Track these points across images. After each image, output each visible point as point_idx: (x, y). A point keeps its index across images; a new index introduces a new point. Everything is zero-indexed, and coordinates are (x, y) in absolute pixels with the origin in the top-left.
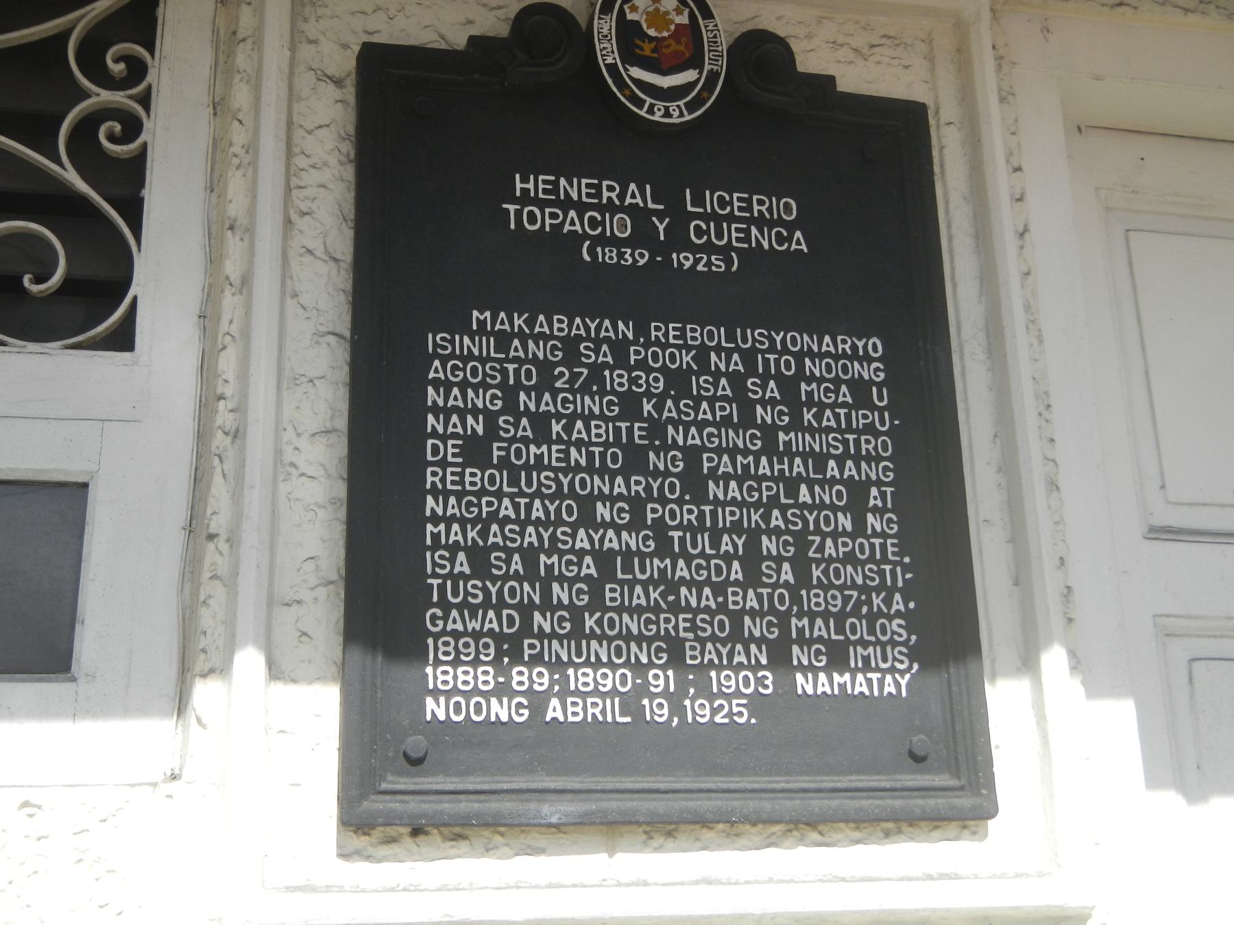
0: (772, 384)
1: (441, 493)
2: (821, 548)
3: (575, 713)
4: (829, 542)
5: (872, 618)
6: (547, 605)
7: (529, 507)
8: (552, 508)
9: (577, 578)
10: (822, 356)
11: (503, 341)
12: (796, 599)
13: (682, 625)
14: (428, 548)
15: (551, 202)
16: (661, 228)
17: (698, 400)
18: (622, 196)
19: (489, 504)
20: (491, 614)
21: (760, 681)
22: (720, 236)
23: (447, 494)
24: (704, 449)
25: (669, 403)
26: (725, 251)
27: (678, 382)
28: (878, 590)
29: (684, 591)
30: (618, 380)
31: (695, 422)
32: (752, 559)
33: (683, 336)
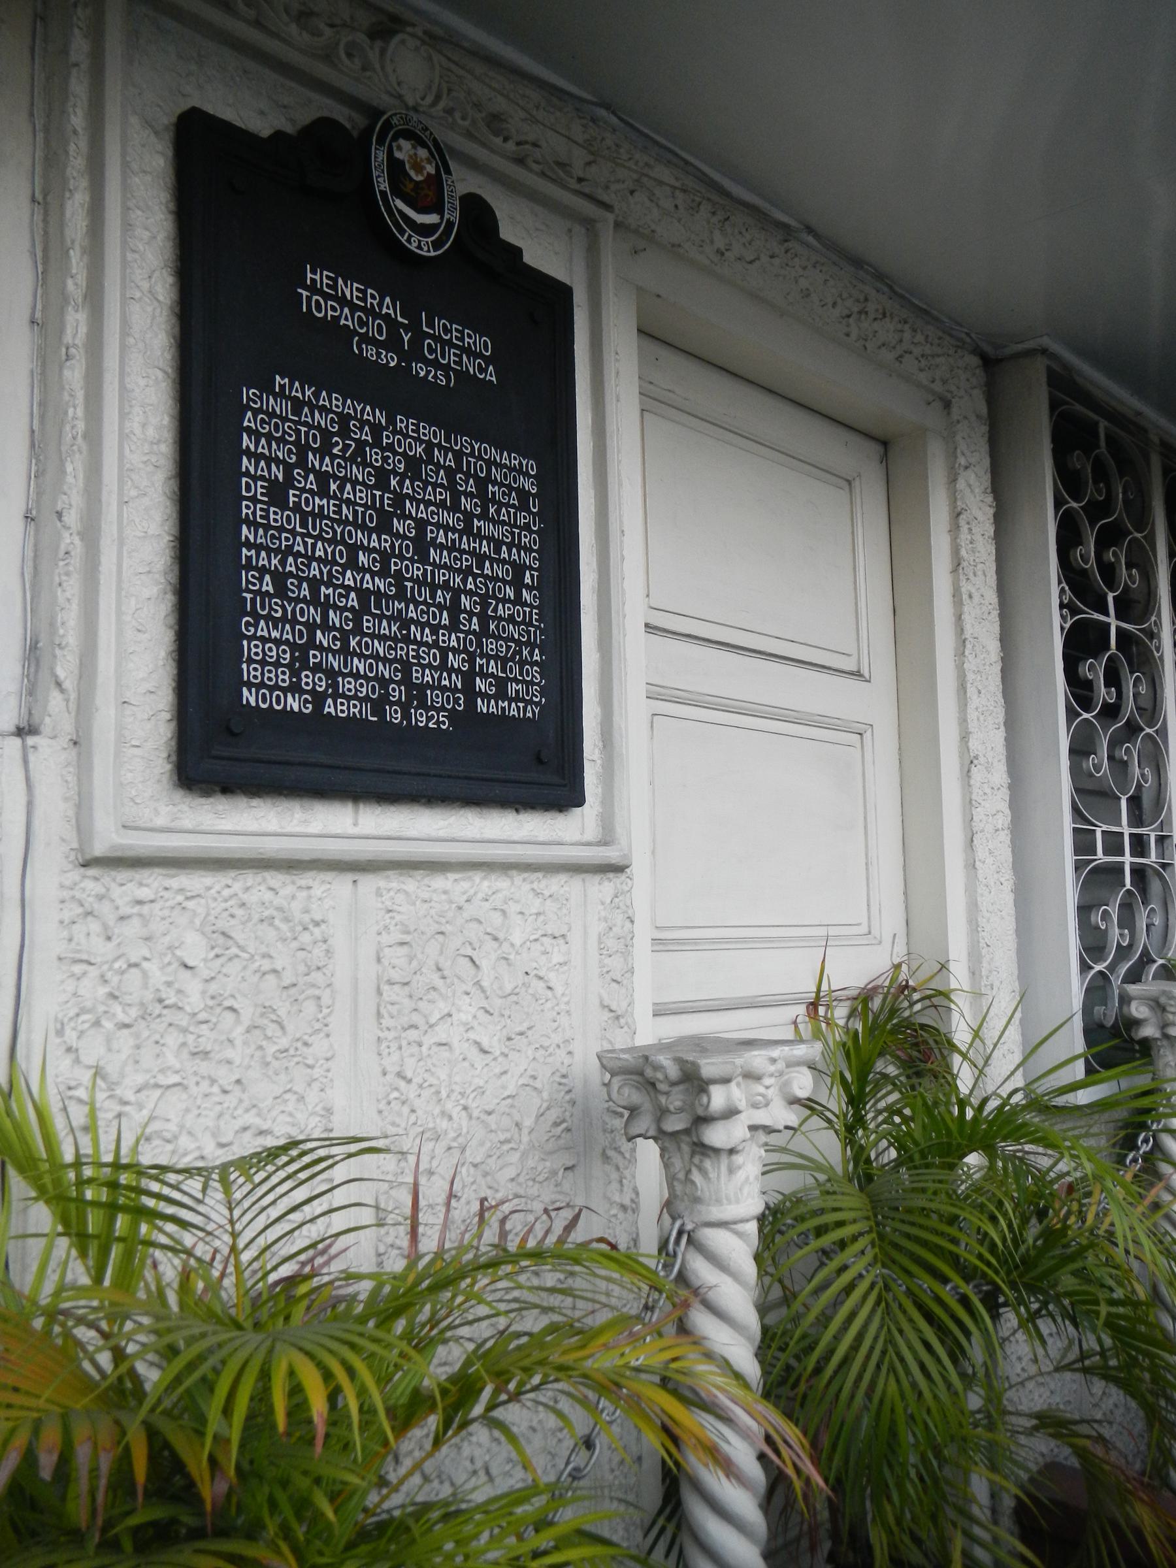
1: (252, 524)
2: (495, 610)
5: (522, 663)
6: (326, 627)
11: (297, 406)
12: (480, 645)
14: (243, 567)
17: (426, 483)
19: (287, 539)
20: (288, 627)
21: (456, 700)
26: (446, 368)
27: (414, 465)
30: (374, 456)
31: (423, 500)
32: (455, 609)
33: (417, 431)
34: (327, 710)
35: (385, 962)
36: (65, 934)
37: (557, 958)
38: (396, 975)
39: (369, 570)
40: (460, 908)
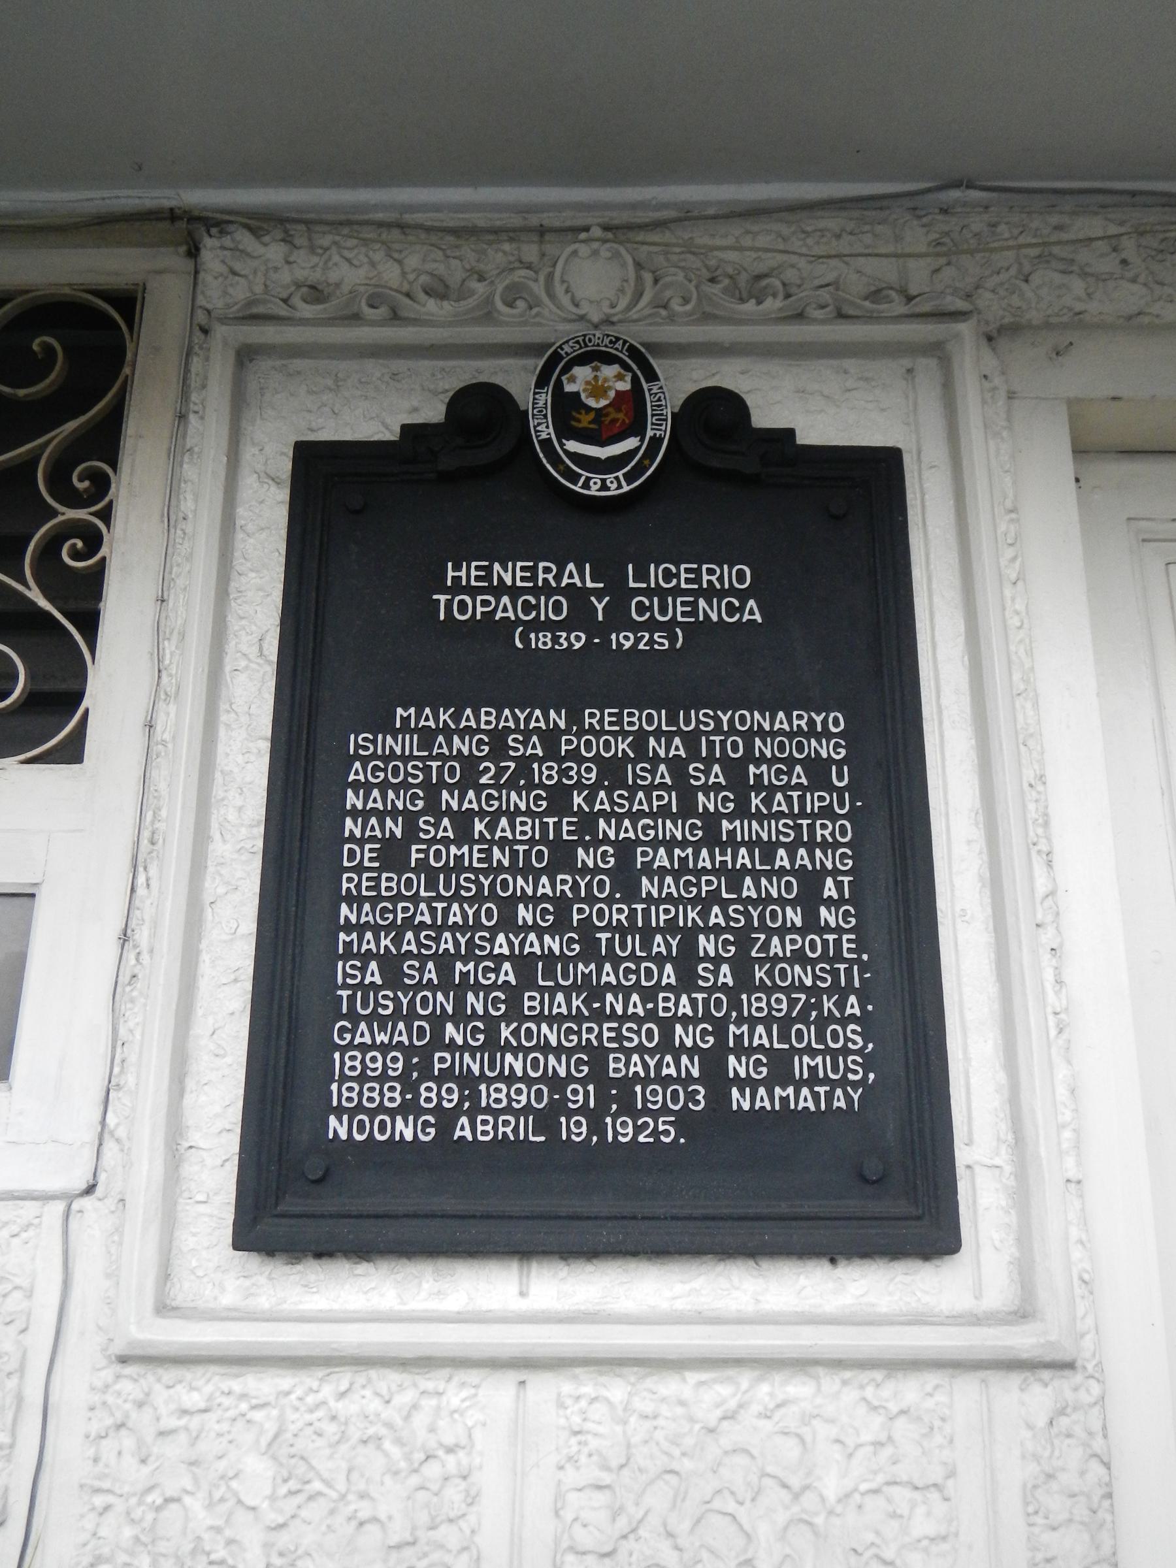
0: (716, 768)
2: (766, 946)
3: (486, 1130)
4: (775, 940)
6: (461, 1016)
7: (446, 911)
8: (470, 913)
9: (494, 986)
10: (773, 734)
11: (427, 737)
12: (735, 1004)
13: (606, 1034)
14: (341, 957)
15: (489, 588)
16: (600, 607)
17: (633, 789)
18: (558, 577)
20: (401, 1026)
21: (691, 1096)
22: (663, 610)
23: (361, 900)
24: (638, 842)
25: (602, 794)
26: (669, 628)
28: (829, 991)
29: (609, 997)
30: (547, 773)
32: (686, 961)
34: (458, 1133)
35: (568, 1516)
36: (91, 1452)
37: (922, 1526)
38: (585, 1539)
39: (535, 927)
40: (711, 1431)
